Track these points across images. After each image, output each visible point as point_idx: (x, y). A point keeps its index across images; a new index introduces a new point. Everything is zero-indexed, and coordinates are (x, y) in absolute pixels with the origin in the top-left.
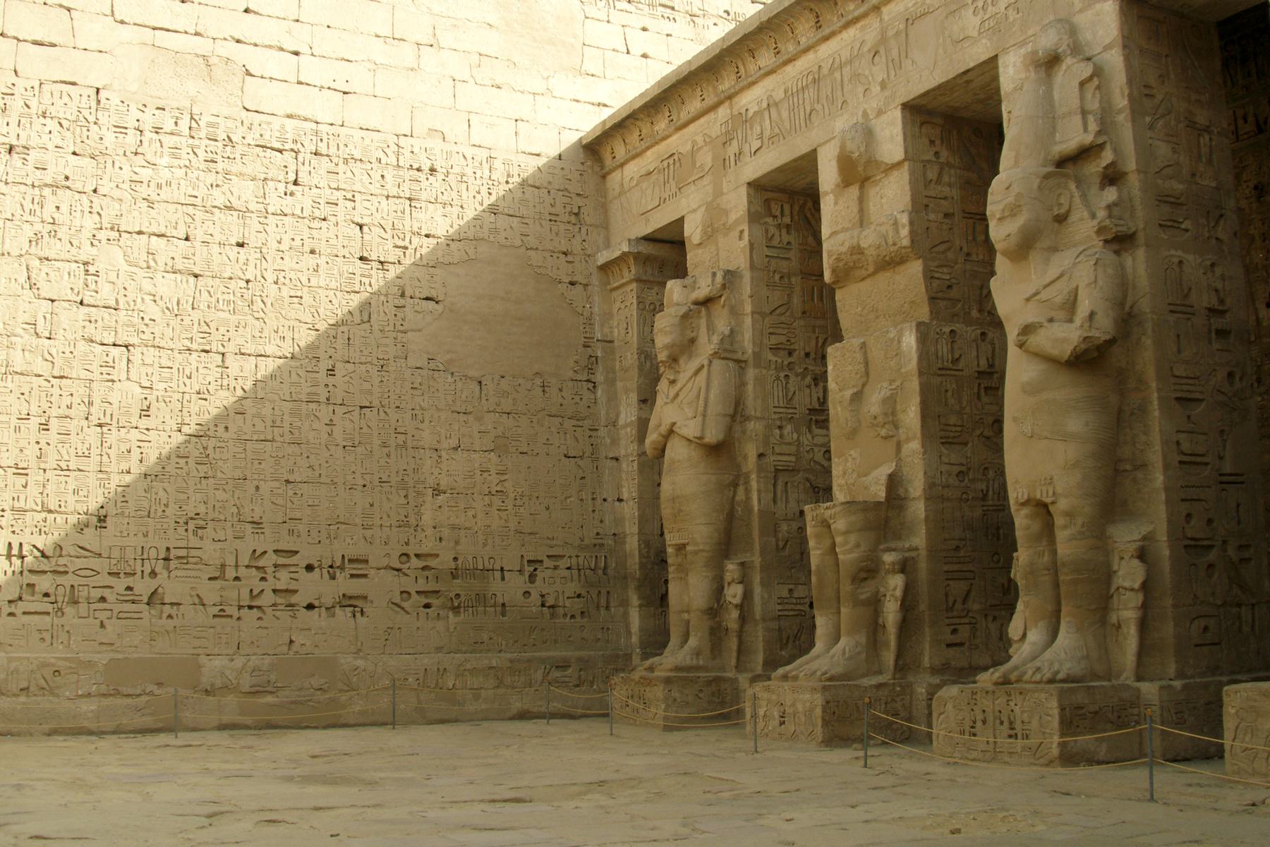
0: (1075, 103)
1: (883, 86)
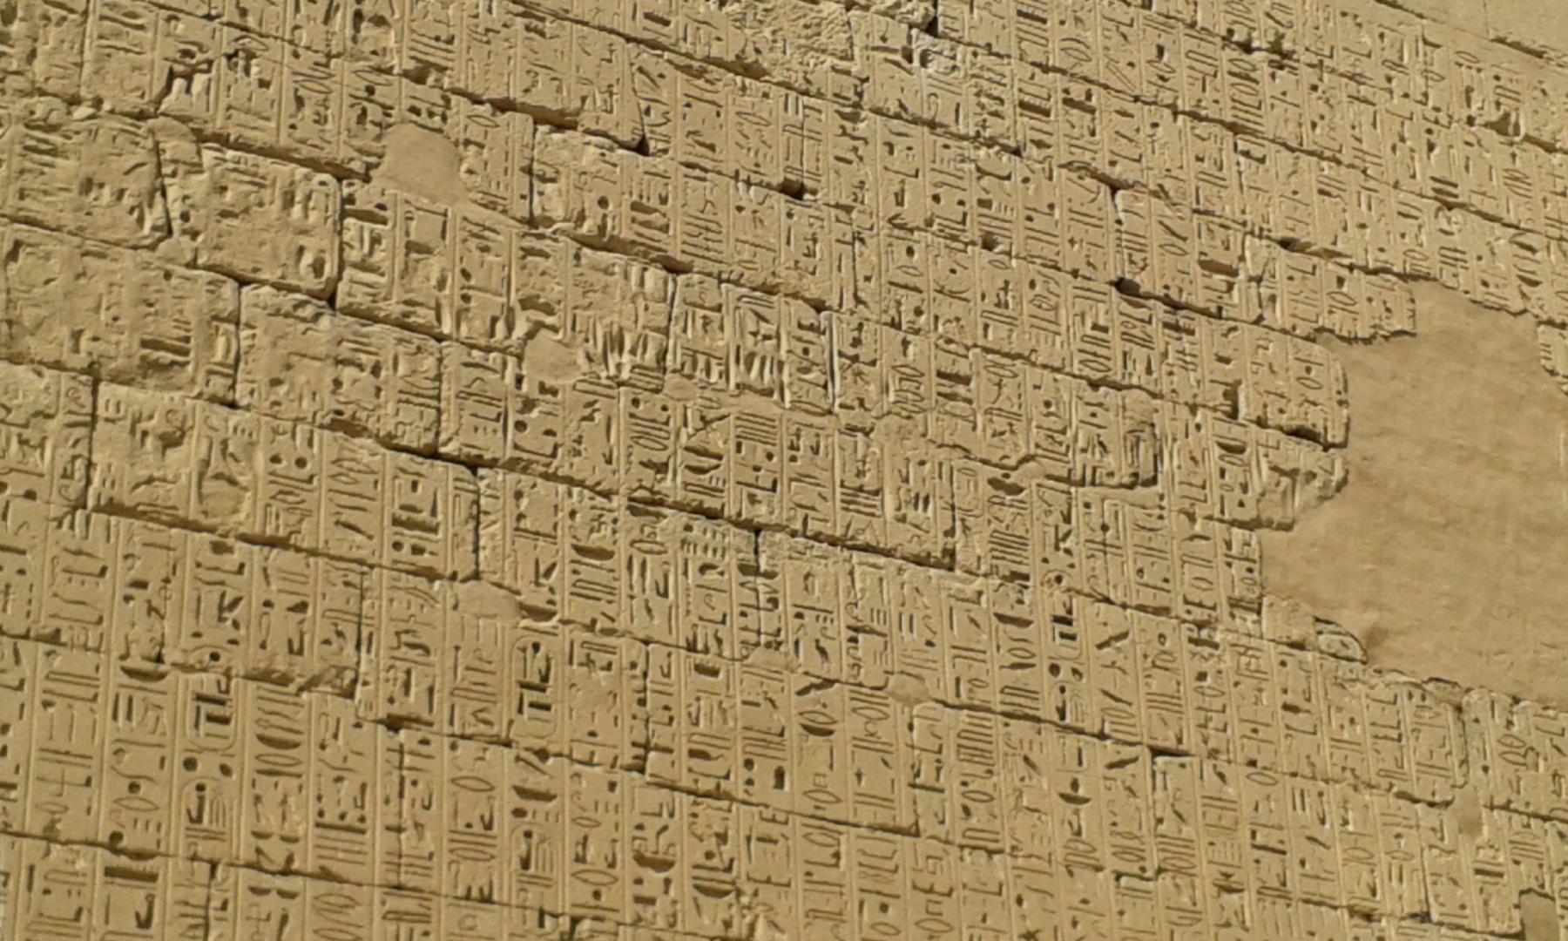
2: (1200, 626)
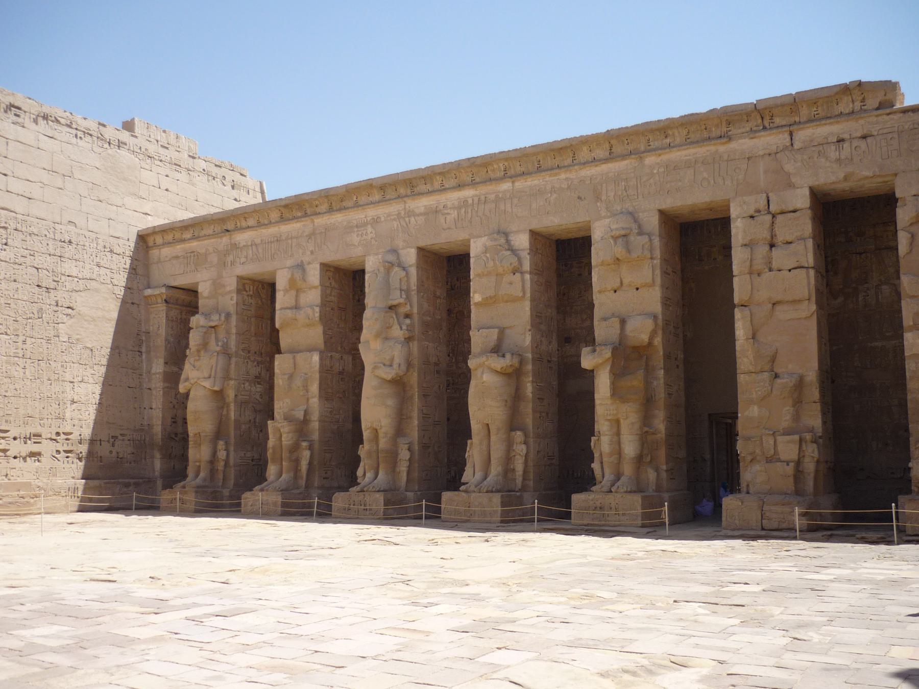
0: (398, 286)
1: (312, 252)
2: (48, 340)
